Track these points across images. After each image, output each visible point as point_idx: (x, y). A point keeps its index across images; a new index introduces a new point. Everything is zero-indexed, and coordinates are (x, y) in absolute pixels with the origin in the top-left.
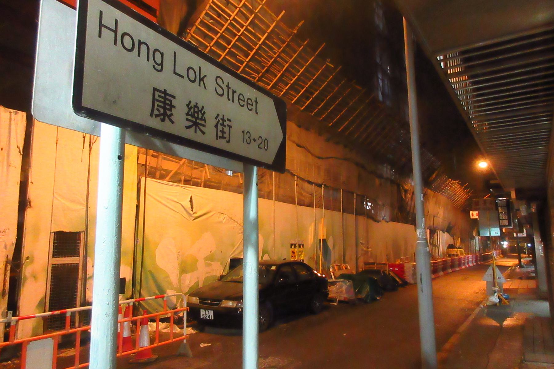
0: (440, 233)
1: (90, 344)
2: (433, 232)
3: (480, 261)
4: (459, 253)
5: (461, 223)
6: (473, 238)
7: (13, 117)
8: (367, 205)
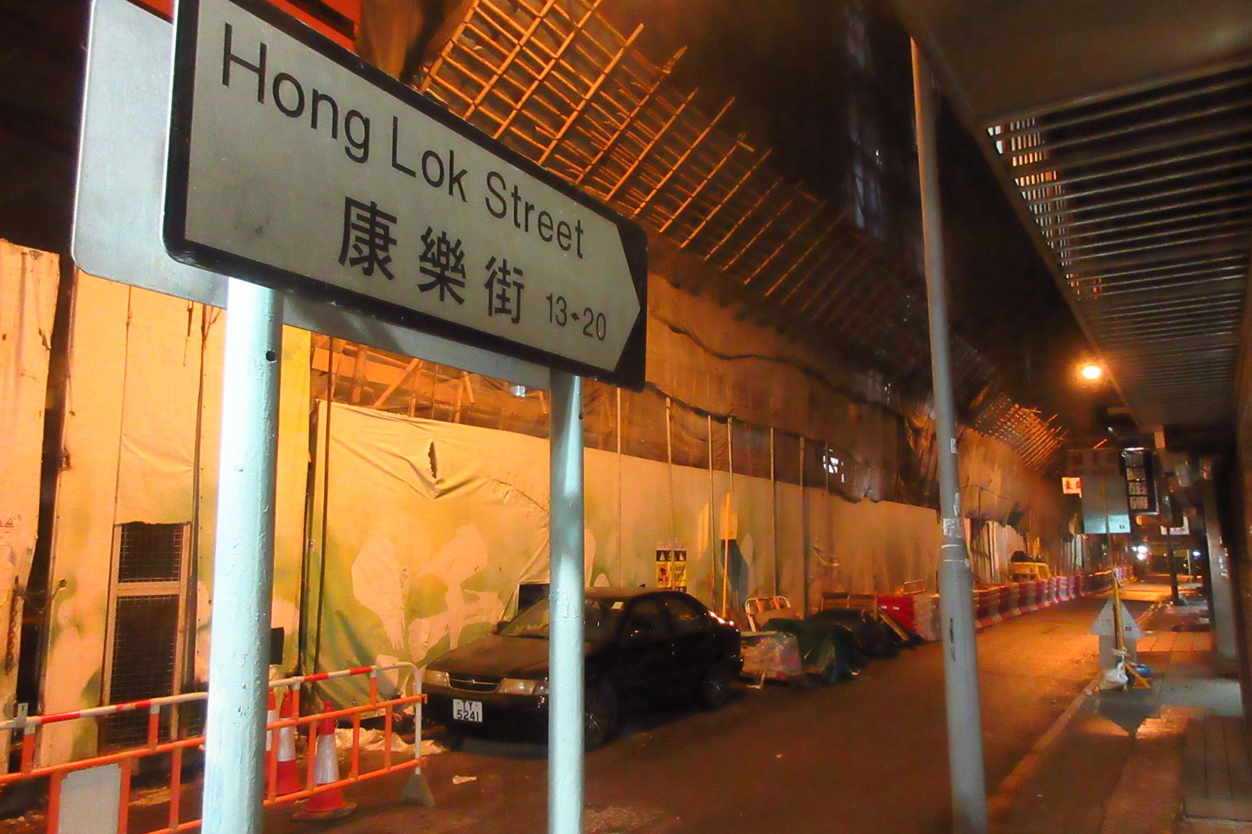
0: (993, 526)
1: (203, 776)
2: (978, 524)
3: (1084, 590)
4: (1037, 571)
5: (1042, 505)
6: (1068, 538)
7: (29, 265)
8: (829, 463)
